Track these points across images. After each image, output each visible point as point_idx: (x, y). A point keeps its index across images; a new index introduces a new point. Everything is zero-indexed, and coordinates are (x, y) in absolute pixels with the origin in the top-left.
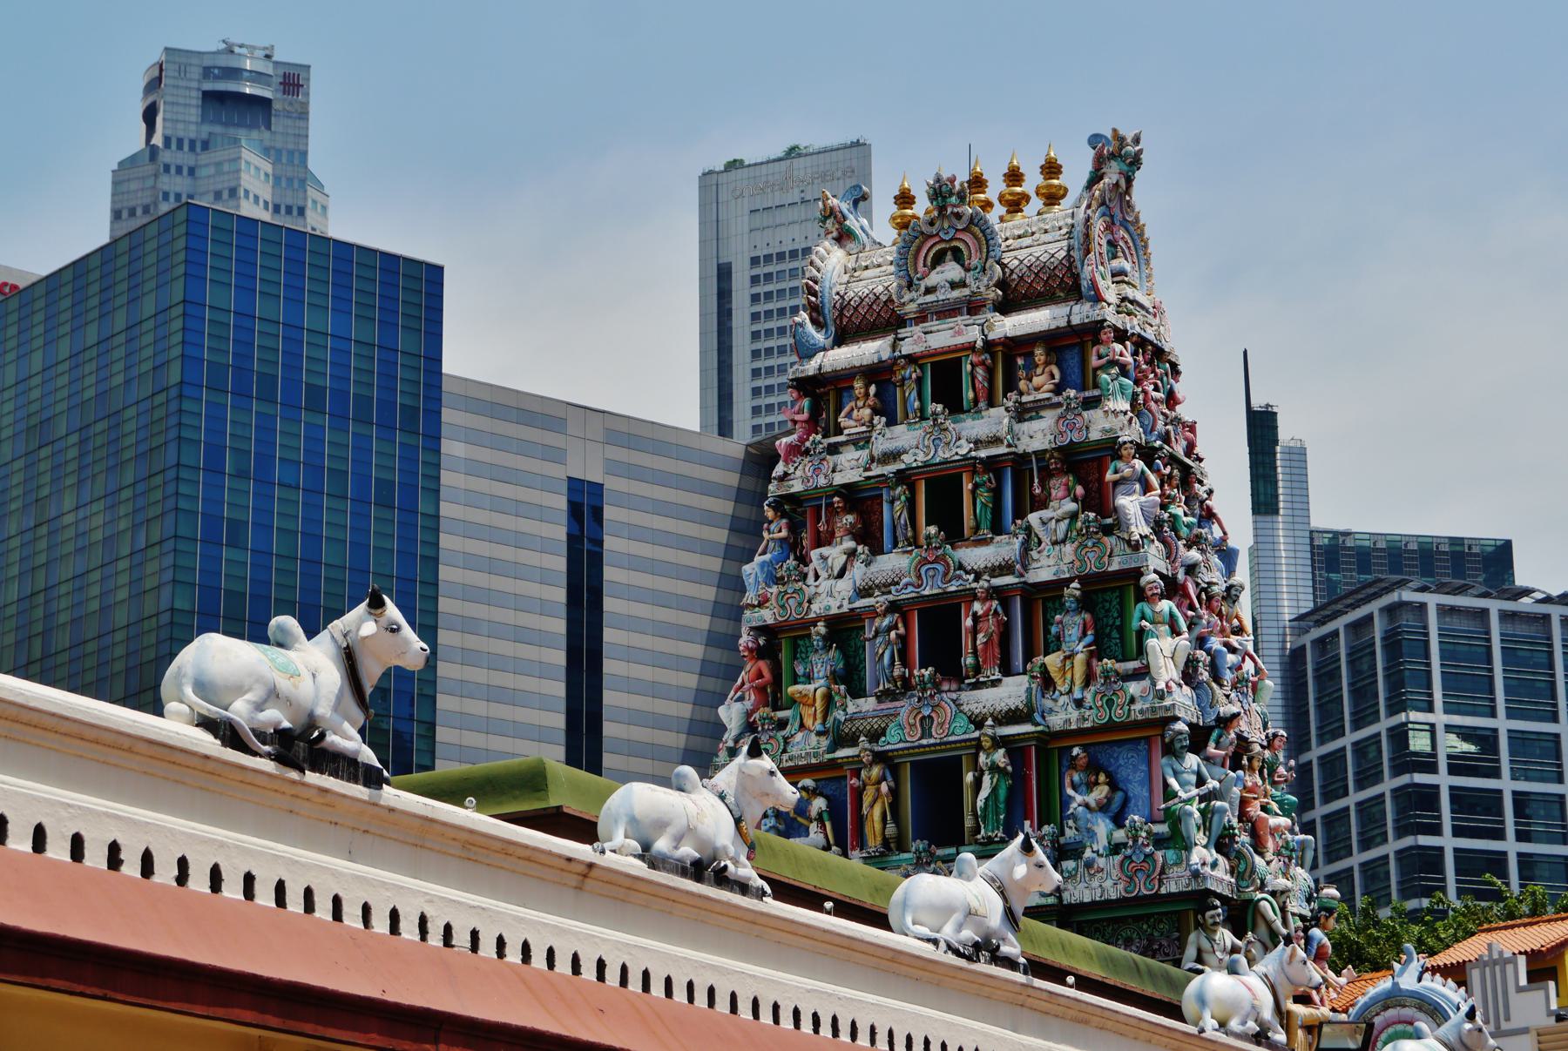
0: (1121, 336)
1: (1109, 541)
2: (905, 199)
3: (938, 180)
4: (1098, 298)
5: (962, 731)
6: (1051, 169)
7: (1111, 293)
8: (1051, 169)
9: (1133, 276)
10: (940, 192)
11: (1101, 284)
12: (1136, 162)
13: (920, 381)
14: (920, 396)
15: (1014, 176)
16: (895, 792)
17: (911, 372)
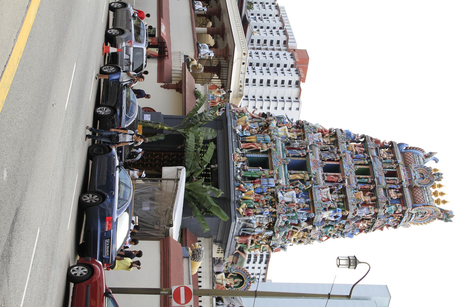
0: (403, 212)
1: (356, 206)
2: (435, 170)
3: (442, 174)
4: (413, 207)
5: (313, 171)
6: (444, 202)
7: (414, 211)
8: (444, 202)
9: (417, 218)
10: (439, 174)
11: (417, 208)
12: (446, 221)
13: (393, 168)
14: (389, 168)
15: (442, 194)
16: (300, 156)
17: (395, 166)
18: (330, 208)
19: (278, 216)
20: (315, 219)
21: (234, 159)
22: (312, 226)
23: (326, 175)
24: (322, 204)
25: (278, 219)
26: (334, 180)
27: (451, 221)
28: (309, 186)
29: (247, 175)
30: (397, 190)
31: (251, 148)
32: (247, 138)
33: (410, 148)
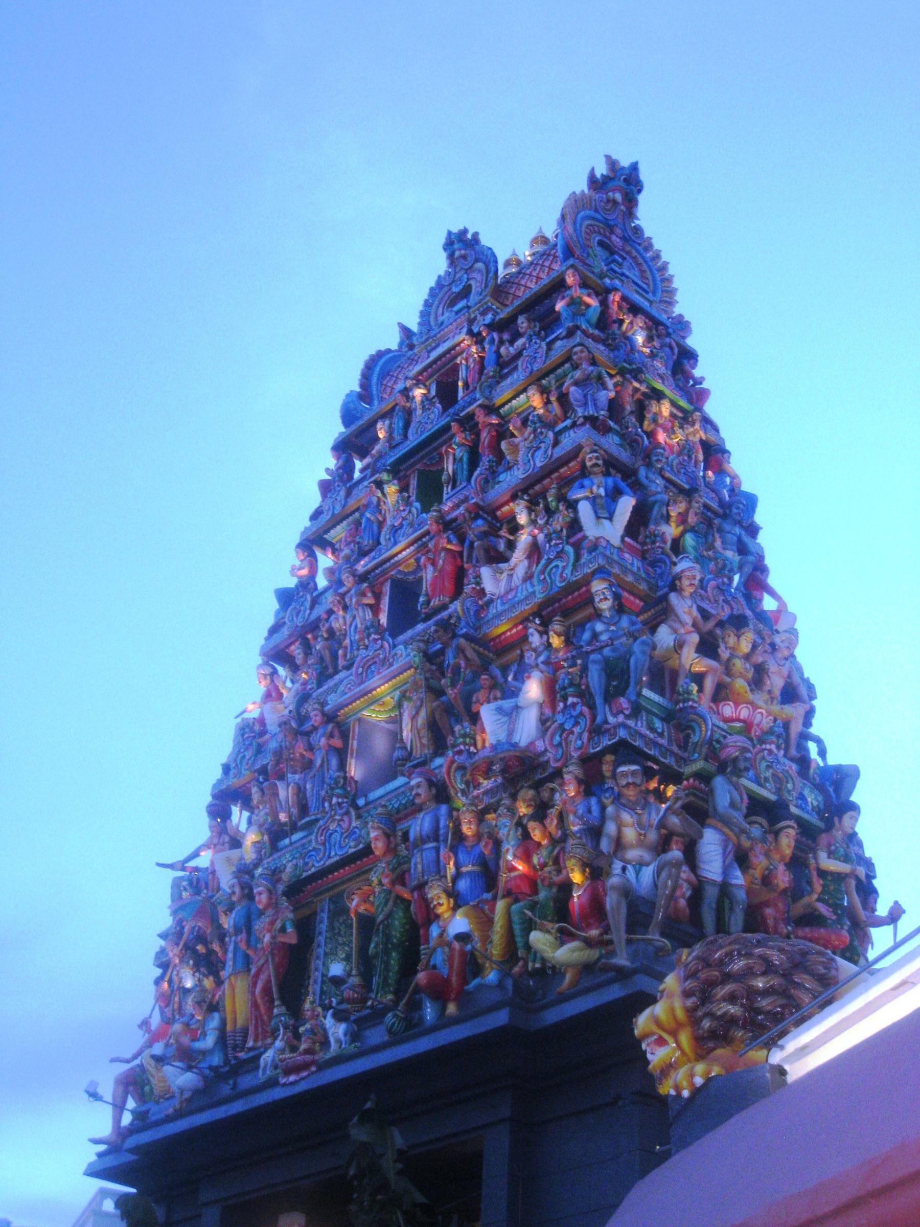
3: (450, 233)
18: (575, 526)
19: (606, 742)
20: (629, 578)
21: (305, 1066)
22: (673, 597)
23: (428, 602)
24: (550, 561)
25: (622, 733)
26: (449, 568)
27: (634, 167)
28: (460, 651)
29: (393, 976)
30: (506, 337)
31: (267, 990)
32: (229, 1027)
33: (362, 386)
